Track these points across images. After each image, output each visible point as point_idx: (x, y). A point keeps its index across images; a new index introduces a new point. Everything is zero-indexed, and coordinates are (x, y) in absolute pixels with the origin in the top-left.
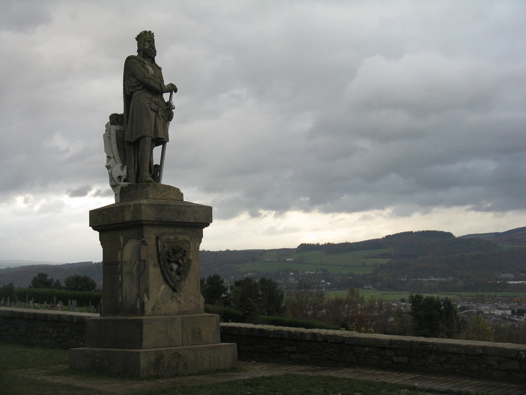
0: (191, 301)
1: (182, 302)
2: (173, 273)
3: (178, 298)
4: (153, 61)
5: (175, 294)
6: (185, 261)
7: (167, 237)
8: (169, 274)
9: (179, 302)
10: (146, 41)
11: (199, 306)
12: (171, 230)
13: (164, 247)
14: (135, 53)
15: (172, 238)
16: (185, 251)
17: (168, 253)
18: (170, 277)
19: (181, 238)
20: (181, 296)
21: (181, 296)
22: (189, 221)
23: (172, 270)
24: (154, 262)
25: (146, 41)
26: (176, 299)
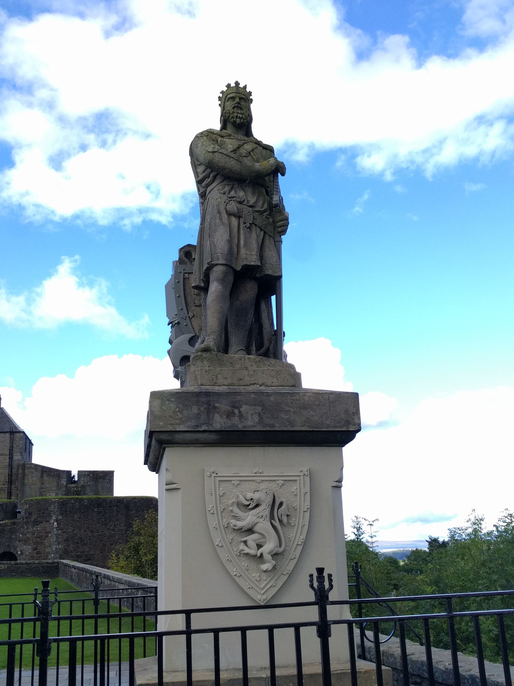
4: (248, 133)
25: (237, 105)
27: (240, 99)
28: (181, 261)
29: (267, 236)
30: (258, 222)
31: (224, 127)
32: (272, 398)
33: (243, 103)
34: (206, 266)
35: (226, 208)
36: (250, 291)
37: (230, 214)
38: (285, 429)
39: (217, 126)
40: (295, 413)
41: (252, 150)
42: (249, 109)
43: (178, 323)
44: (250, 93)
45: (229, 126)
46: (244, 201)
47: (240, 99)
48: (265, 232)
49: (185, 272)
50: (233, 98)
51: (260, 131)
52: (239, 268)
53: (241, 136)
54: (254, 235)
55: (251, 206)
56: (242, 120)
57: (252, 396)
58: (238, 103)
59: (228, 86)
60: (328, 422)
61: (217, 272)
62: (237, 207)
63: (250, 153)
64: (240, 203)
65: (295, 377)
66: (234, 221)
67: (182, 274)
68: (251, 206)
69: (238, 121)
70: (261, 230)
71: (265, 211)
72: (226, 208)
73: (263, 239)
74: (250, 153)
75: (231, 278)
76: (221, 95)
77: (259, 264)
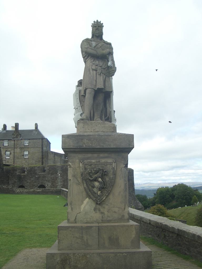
0: (115, 212)
1: (106, 213)
2: (95, 190)
3: (102, 210)
4: (101, 39)
5: (98, 206)
6: (107, 179)
7: (89, 160)
8: (90, 191)
9: (102, 213)
10: (98, 28)
11: (123, 216)
12: (96, 155)
13: (86, 169)
15: (93, 161)
16: (106, 171)
17: (89, 173)
18: (91, 193)
19: (103, 161)
20: (104, 208)
21: (104, 208)
22: (109, 147)
23: (93, 187)
24: (78, 181)
25: (98, 28)
26: (99, 210)
27: (98, 26)
28: (78, 86)
29: (107, 77)
30: (103, 72)
31: (93, 37)
33: (99, 28)
34: (84, 89)
35: (92, 68)
37: (93, 70)
39: (90, 37)
41: (102, 46)
42: (102, 30)
43: (77, 108)
44: (102, 24)
45: (94, 37)
46: (98, 65)
47: (98, 26)
48: (106, 76)
49: (80, 89)
50: (96, 26)
51: (106, 38)
52: (96, 89)
53: (98, 40)
54: (102, 77)
55: (100, 67)
56: (99, 35)
57: (96, 136)
58: (97, 28)
59: (94, 22)
61: (88, 91)
62: (95, 67)
64: (97, 65)
65: (114, 128)
66: (95, 72)
67: (79, 90)
68: (100, 67)
69: (97, 35)
70: (105, 75)
71: (106, 68)
72: (92, 68)
73: (105, 78)
74: (101, 47)
75: (93, 93)
76: (92, 25)
77: (103, 88)
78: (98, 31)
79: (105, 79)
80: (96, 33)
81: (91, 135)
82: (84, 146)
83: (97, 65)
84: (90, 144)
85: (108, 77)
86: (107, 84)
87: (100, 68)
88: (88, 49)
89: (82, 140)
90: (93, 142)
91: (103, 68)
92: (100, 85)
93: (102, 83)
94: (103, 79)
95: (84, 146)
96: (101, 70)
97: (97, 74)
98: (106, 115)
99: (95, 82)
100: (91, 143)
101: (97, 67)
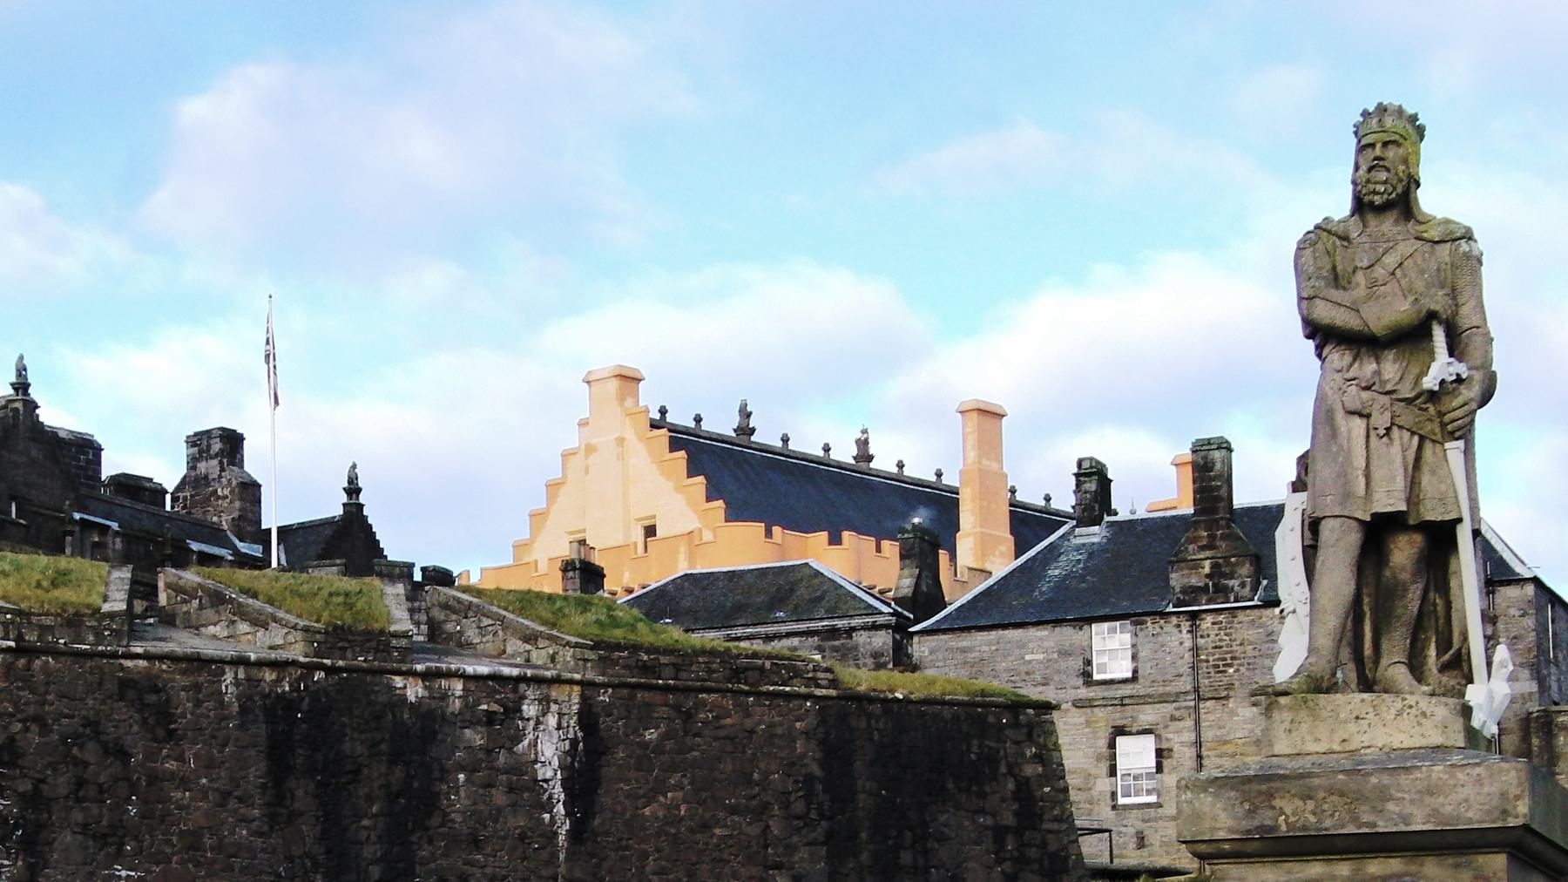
14: (1339, 205)
29: (1428, 445)
32: (1374, 780)
36: (1403, 552)
38: (1394, 829)
40: (1412, 802)
42: (1411, 161)
47: (1385, 144)
48: (1422, 438)
51: (1436, 199)
54: (1396, 449)
59: (1365, 114)
60: (1470, 814)
61: (1328, 530)
63: (1393, 274)
66: (1358, 425)
70: (1413, 433)
74: (1393, 274)
77: (1404, 508)
78: (1383, 176)
79: (1418, 458)
80: (1371, 187)
81: (1309, 775)
82: (1284, 828)
83: (1368, 388)
84: (1312, 819)
85: (1434, 441)
86: (1426, 480)
87: (1385, 399)
88: (1317, 301)
89: (1271, 796)
90: (1326, 807)
91: (1401, 400)
92: (1389, 499)
93: (1400, 483)
94: (1404, 458)
95: (1284, 828)
96: (1388, 415)
97: (1373, 433)
98: (1444, 644)
99: (1362, 481)
100: (1314, 813)
101: (1365, 395)
